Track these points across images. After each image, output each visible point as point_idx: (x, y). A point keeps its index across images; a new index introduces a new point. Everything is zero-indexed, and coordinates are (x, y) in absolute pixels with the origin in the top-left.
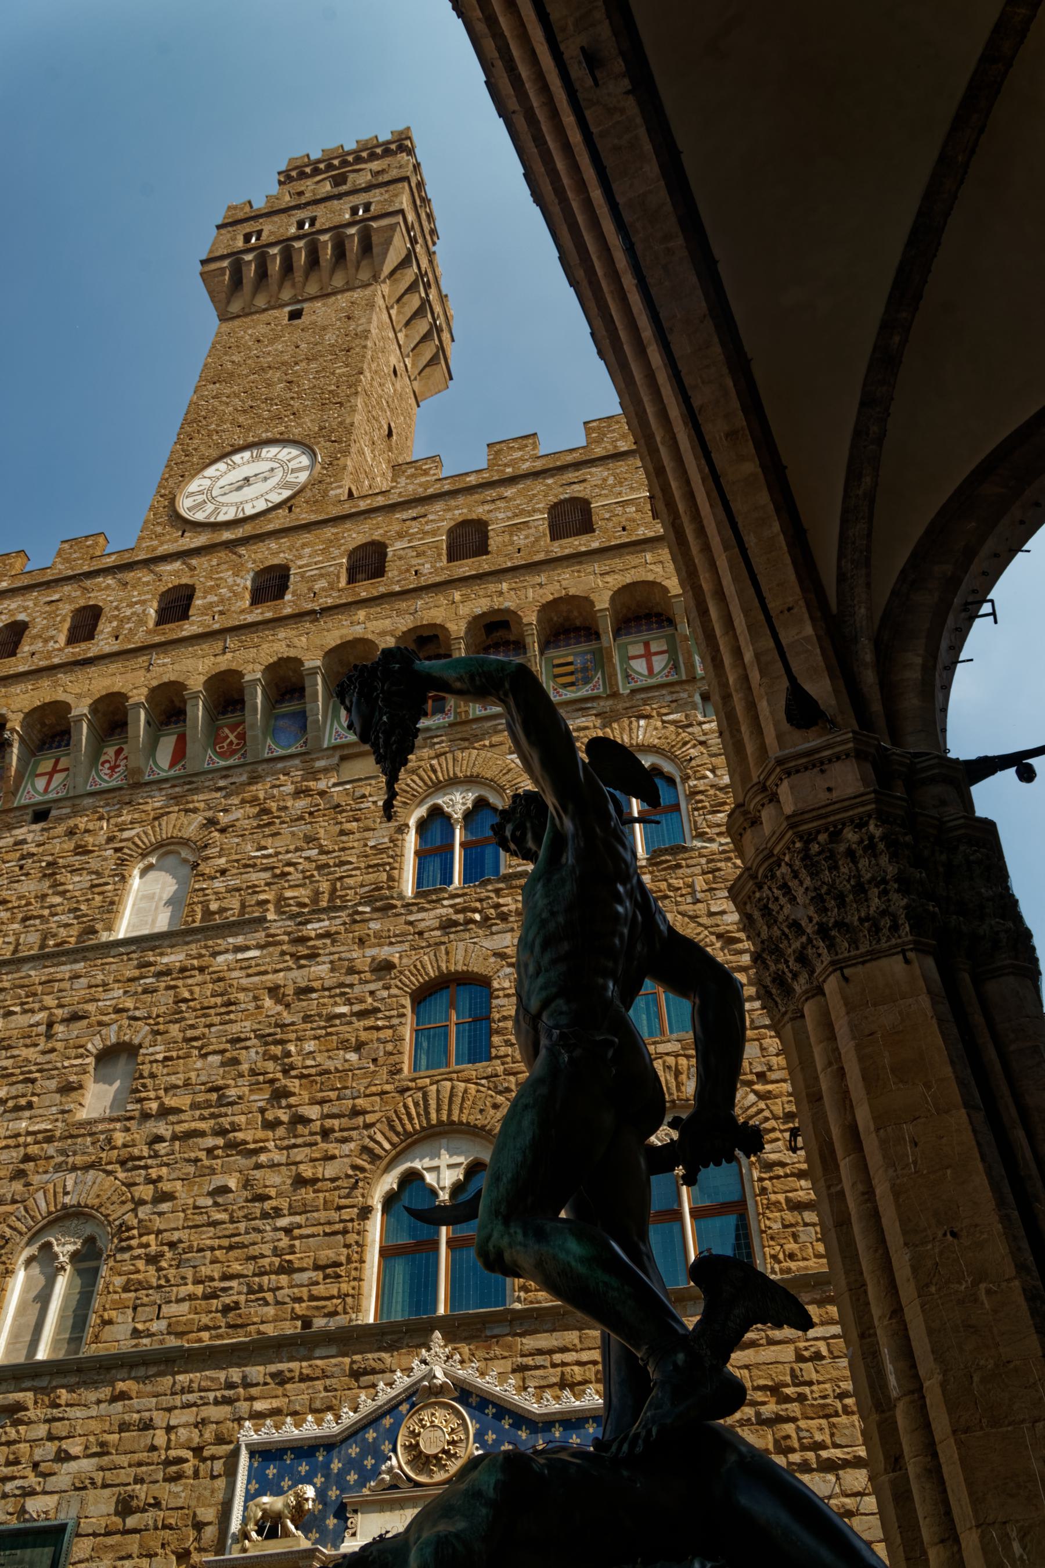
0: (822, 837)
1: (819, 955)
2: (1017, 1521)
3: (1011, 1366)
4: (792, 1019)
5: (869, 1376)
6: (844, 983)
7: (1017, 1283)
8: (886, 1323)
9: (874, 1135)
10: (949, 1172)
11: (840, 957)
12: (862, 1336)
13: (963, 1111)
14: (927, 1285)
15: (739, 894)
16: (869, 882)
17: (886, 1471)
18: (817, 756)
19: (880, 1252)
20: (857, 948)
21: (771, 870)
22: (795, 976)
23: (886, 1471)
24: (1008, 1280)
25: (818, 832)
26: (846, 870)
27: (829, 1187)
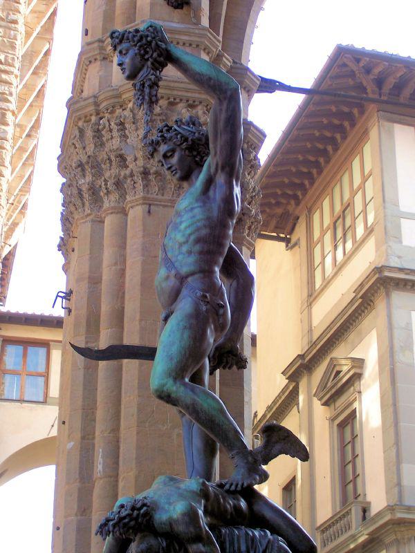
1: (134, 187)
5: (81, 462)
8: (105, 435)
9: (137, 323)
11: (149, 196)
12: (83, 438)
15: (78, 110)
18: (177, 36)
19: (115, 393)
20: (163, 195)
22: (108, 193)
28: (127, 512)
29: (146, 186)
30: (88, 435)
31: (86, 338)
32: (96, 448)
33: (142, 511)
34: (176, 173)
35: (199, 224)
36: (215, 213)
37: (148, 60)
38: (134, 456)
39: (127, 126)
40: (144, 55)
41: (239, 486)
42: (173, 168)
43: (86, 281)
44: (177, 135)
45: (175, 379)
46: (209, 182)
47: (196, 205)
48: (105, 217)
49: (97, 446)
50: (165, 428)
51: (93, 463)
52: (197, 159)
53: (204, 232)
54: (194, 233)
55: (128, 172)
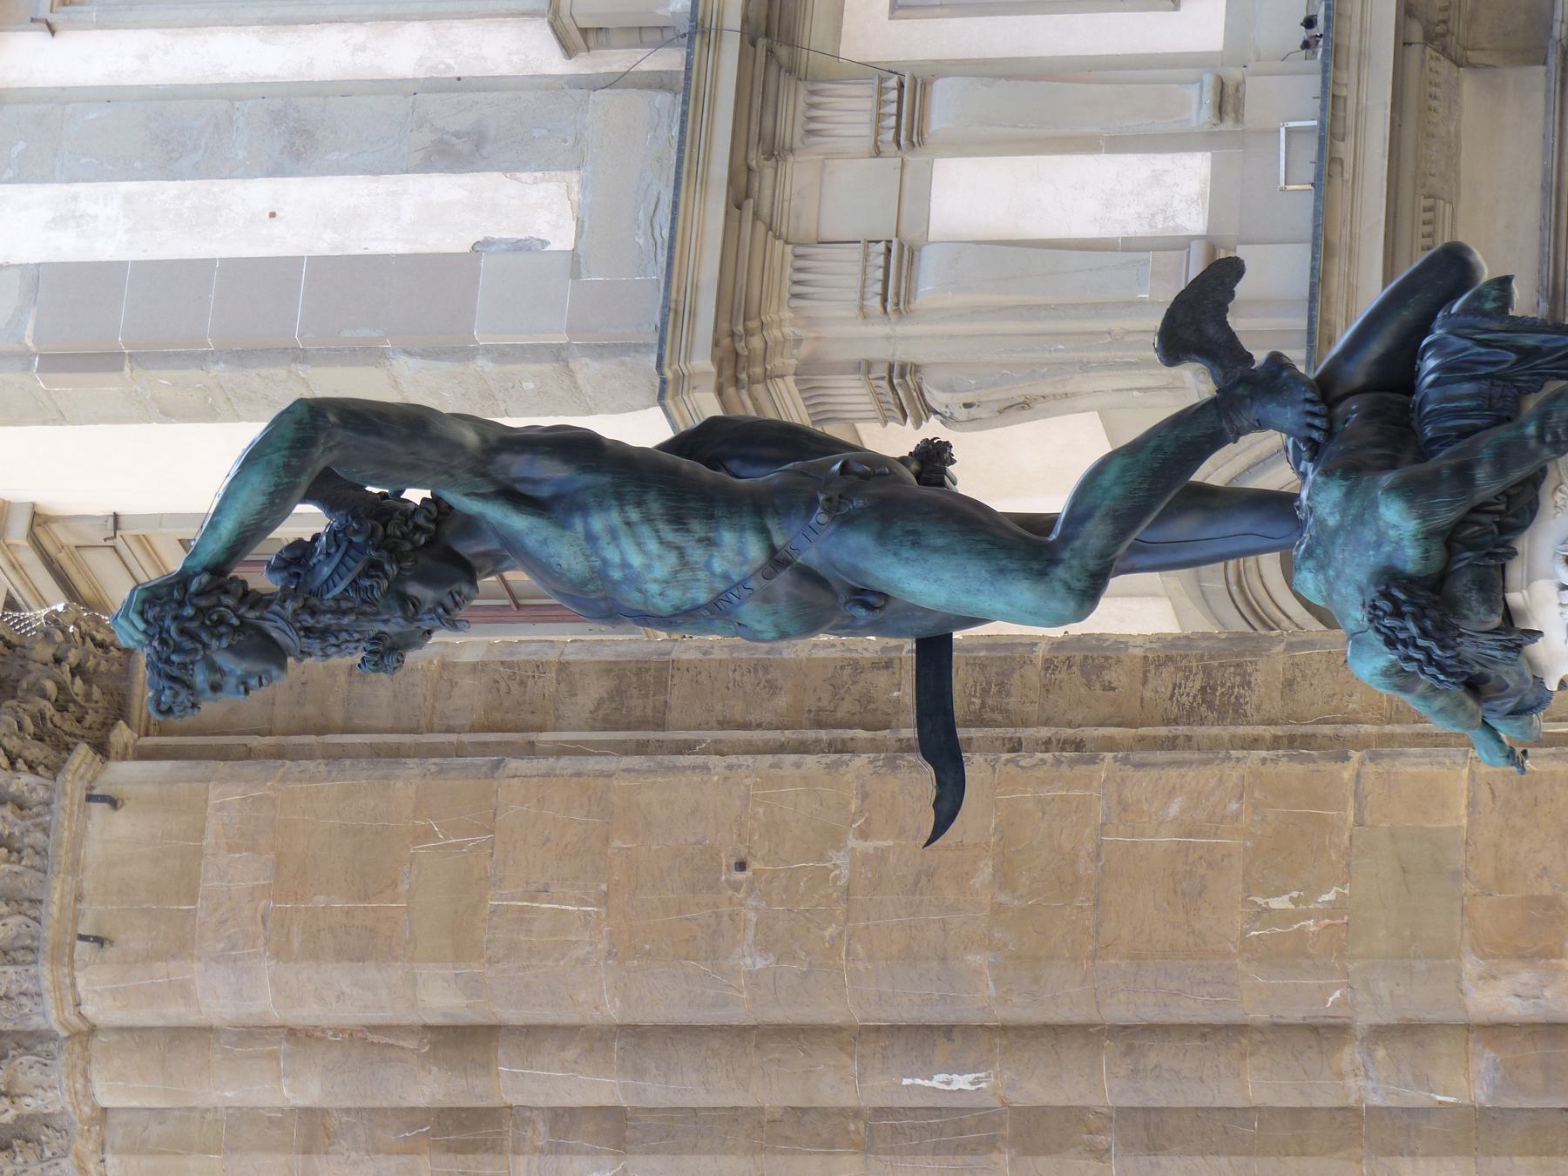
5: (936, 1150)
6: (110, 952)
28: (1411, 625)
31: (517, 1152)
33: (1403, 597)
34: (459, 594)
36: (604, 479)
41: (1315, 409)
42: (449, 603)
45: (1054, 562)
46: (513, 496)
47: (578, 524)
48: (94, 1107)
51: (938, 1110)
52: (423, 541)
53: (655, 507)
54: (657, 531)
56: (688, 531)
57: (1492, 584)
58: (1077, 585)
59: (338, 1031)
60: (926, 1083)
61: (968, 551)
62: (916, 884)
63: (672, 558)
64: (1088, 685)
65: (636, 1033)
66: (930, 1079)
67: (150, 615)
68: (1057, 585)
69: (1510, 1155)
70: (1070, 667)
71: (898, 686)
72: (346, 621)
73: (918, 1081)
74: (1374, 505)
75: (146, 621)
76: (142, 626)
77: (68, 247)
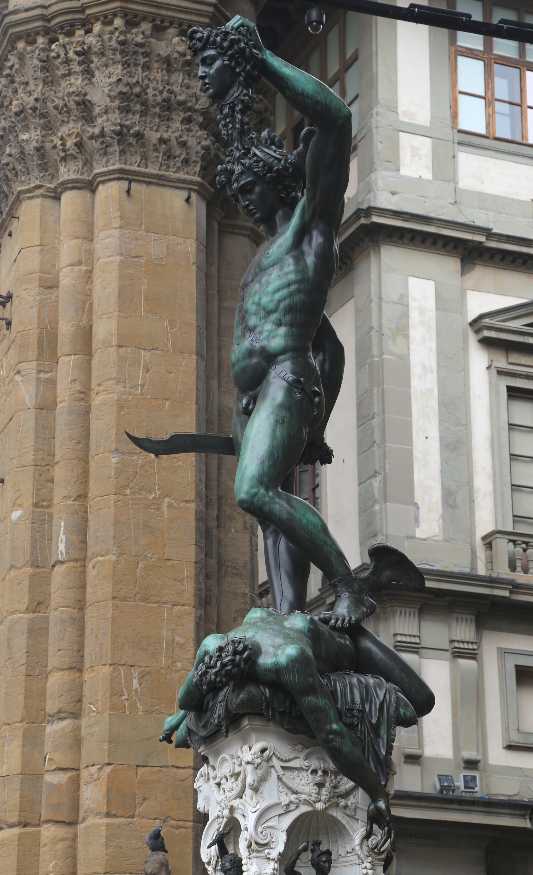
0: (146, 26)
2: (141, 667)
3: (171, 562)
4: (43, 196)
5: (33, 538)
6: (125, 195)
7: (193, 505)
8: (69, 503)
10: (168, 403)
11: (127, 167)
12: (36, 505)
13: (195, 357)
14: (124, 487)
16: (180, 104)
17: (27, 610)
19: (81, 446)
21: (72, 25)
23: (27, 610)
24: (187, 501)
25: (144, 18)
26: (159, 76)
27: (39, 372)
28: (229, 658)
29: (122, 152)
30: (44, 501)
31: (38, 365)
32: (55, 521)
33: (245, 655)
35: (293, 288)
37: (239, 74)
38: (112, 534)
39: (95, 59)
40: (235, 68)
41: (346, 621)
43: (37, 283)
44: (257, 162)
45: (267, 489)
48: (61, 193)
49: (55, 516)
50: (152, 496)
51: (50, 540)
53: (297, 298)
54: (285, 299)
55: (97, 131)
56: (285, 315)
57: (255, 710)
58: (255, 500)
59: (91, 290)
60: (62, 532)
61: (273, 447)
62: (148, 527)
63: (271, 306)
64: (236, 611)
65: (88, 411)
66: (63, 534)
67: (242, 29)
68: (255, 490)
69: (21, 790)
70: (244, 603)
71: (236, 531)
72: (238, 126)
73: (62, 529)
74: (296, 643)
75: (238, 27)
76: (235, 26)
77: (416, 369)
